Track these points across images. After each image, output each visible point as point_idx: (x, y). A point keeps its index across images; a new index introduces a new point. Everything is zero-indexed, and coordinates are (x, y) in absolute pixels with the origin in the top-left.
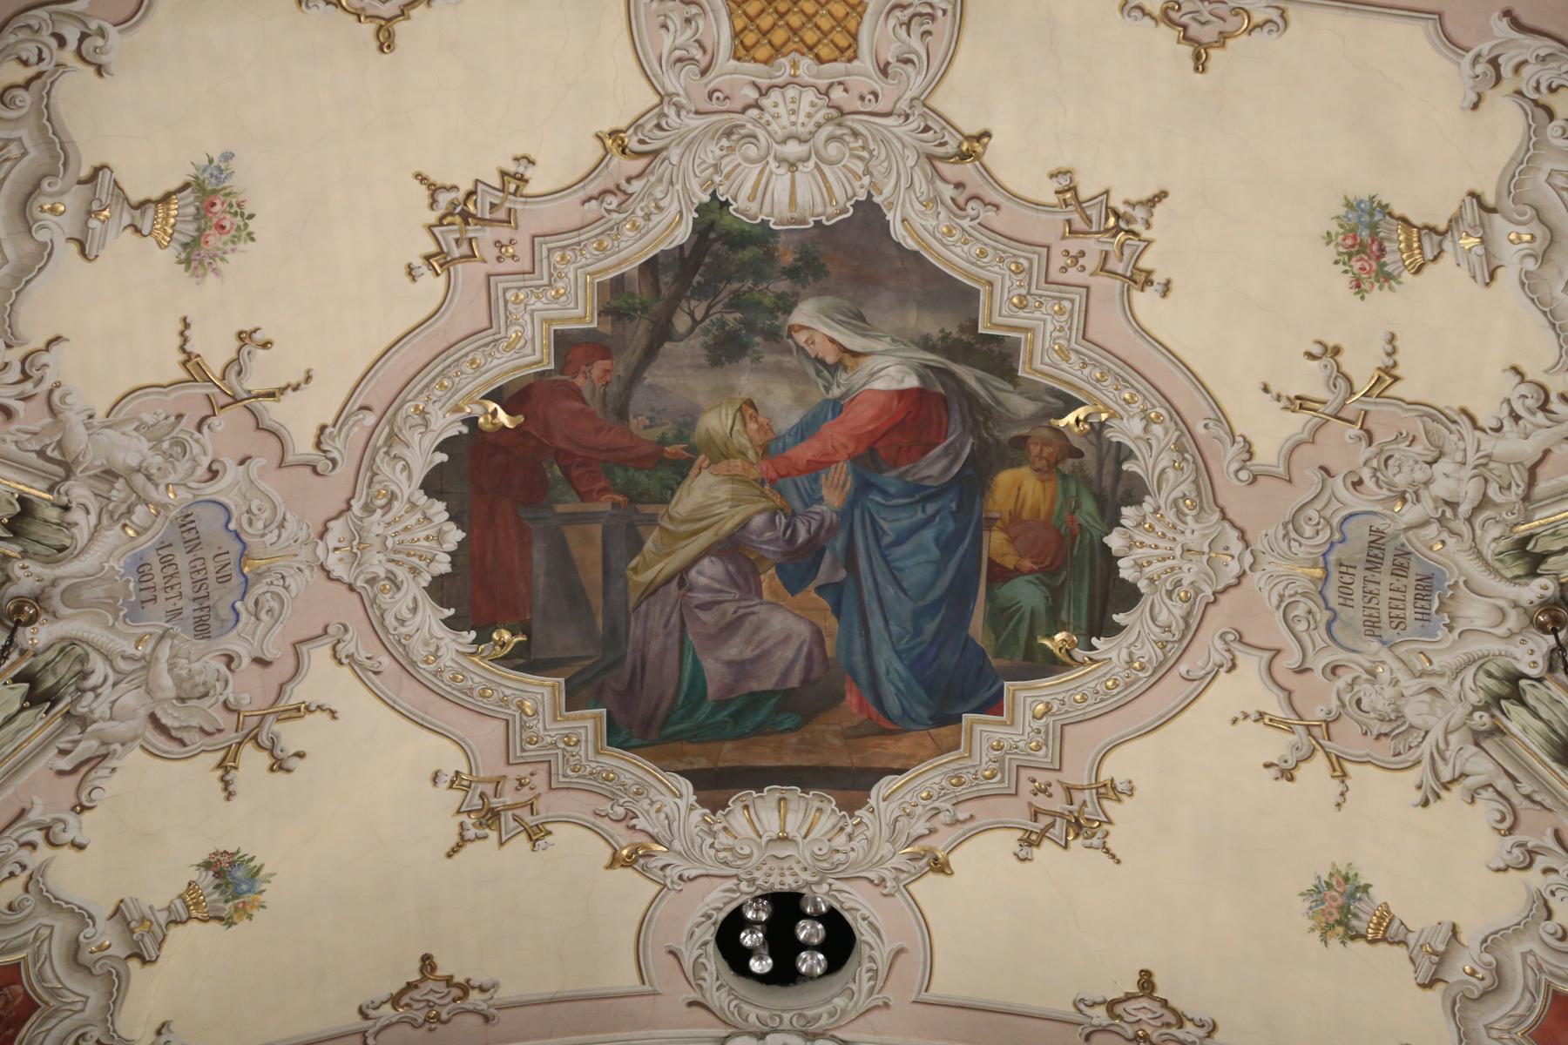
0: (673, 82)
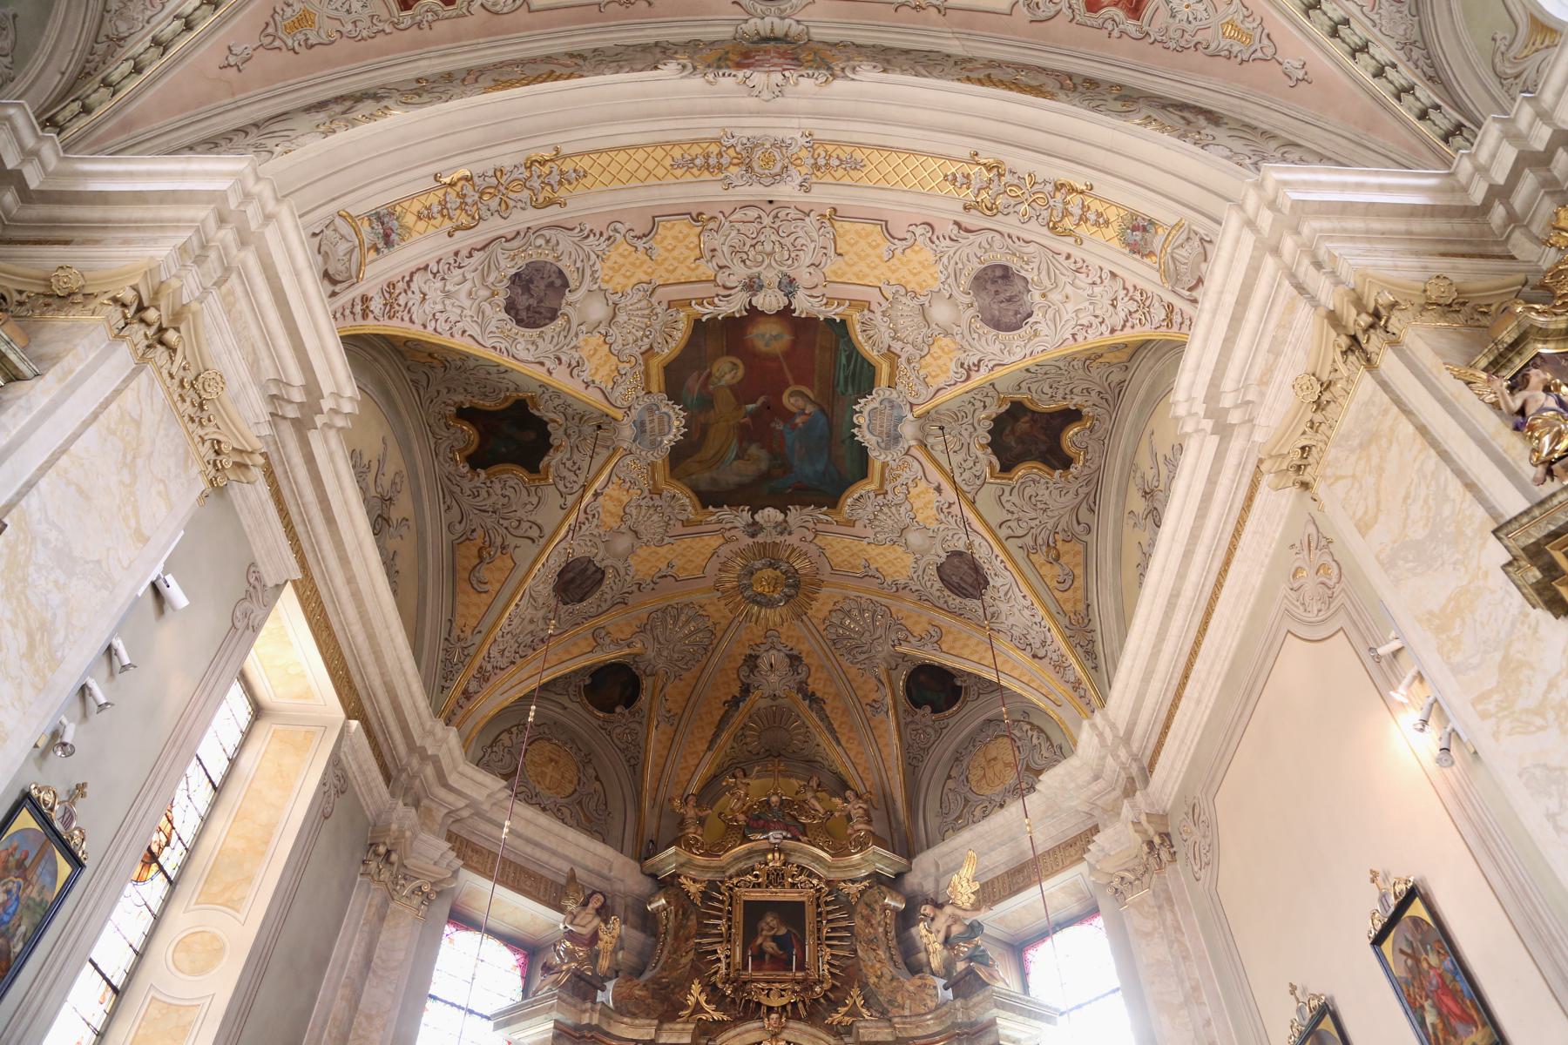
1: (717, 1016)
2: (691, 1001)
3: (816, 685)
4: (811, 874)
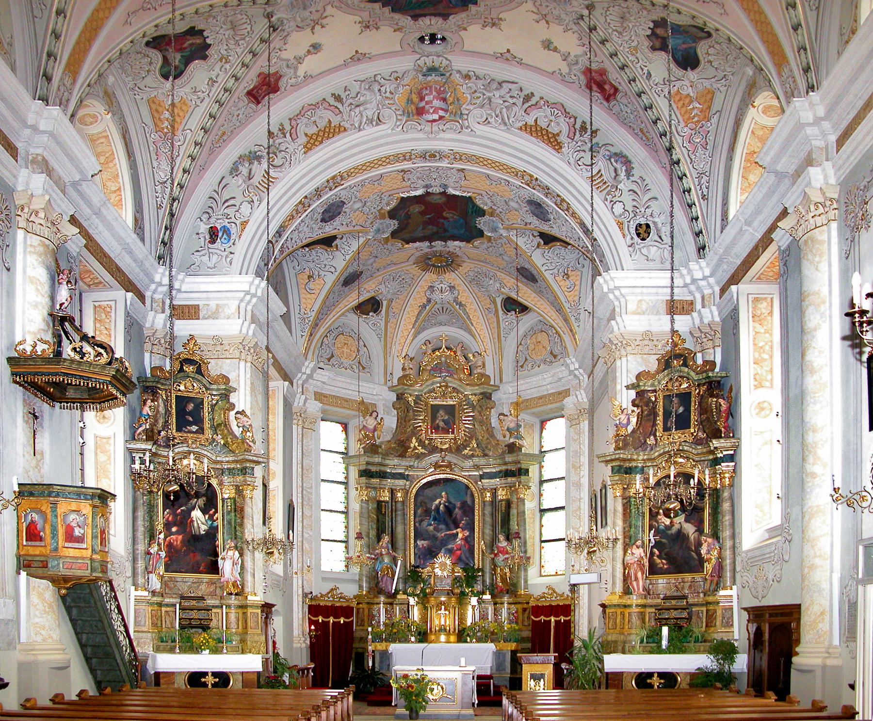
2: (412, 445)
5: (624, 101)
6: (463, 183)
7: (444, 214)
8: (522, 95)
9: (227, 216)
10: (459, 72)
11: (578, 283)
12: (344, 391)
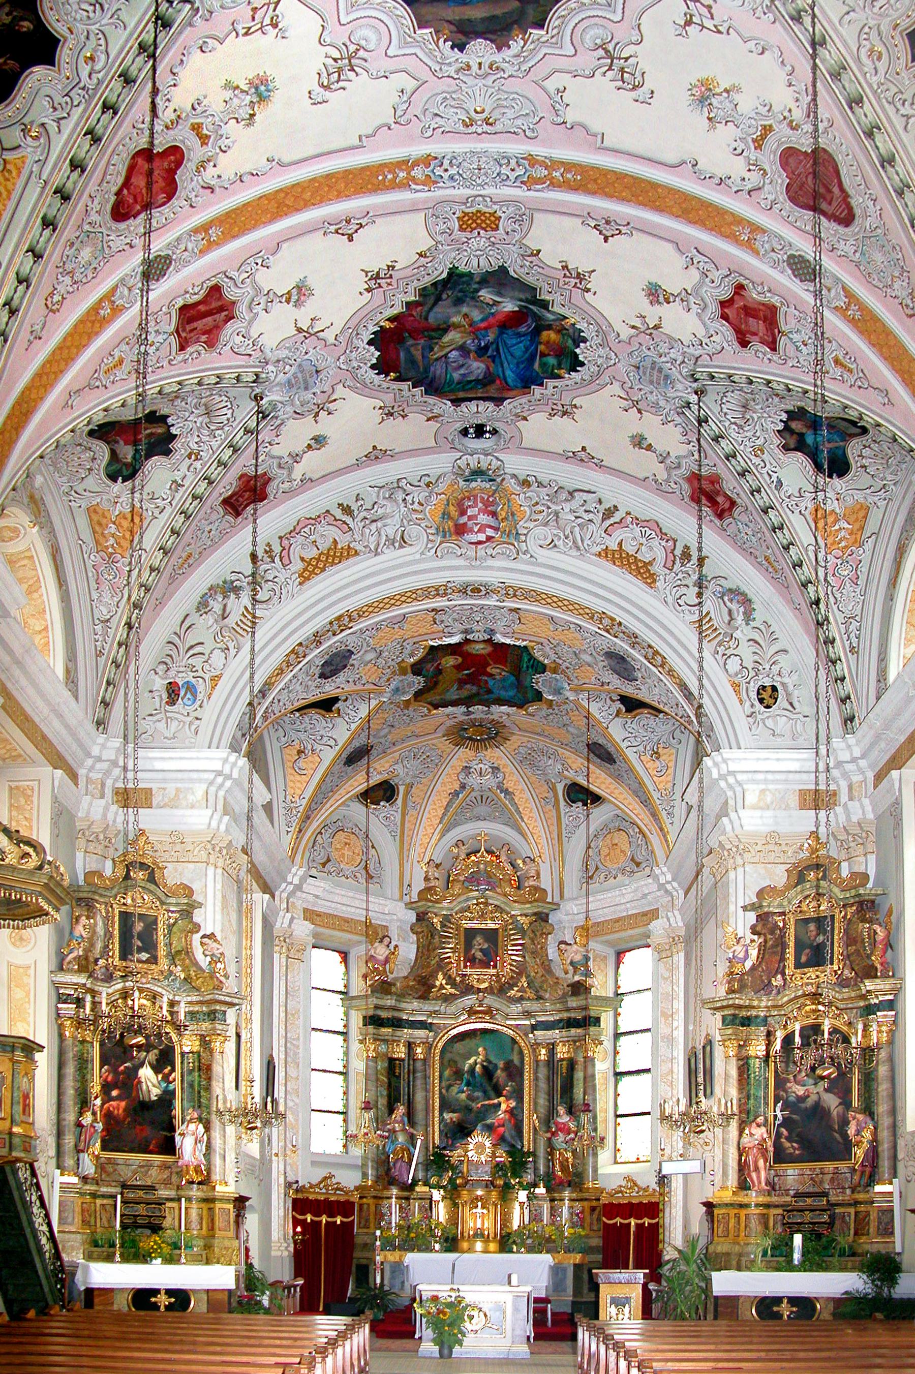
0: (439, 238)
1: (453, 991)
2: (438, 983)
3: (509, 785)
4: (502, 911)
5: (744, 518)
6: (516, 627)
7: (488, 669)
8: (602, 508)
9: (192, 669)
10: (514, 476)
11: (671, 764)
12: (344, 908)
